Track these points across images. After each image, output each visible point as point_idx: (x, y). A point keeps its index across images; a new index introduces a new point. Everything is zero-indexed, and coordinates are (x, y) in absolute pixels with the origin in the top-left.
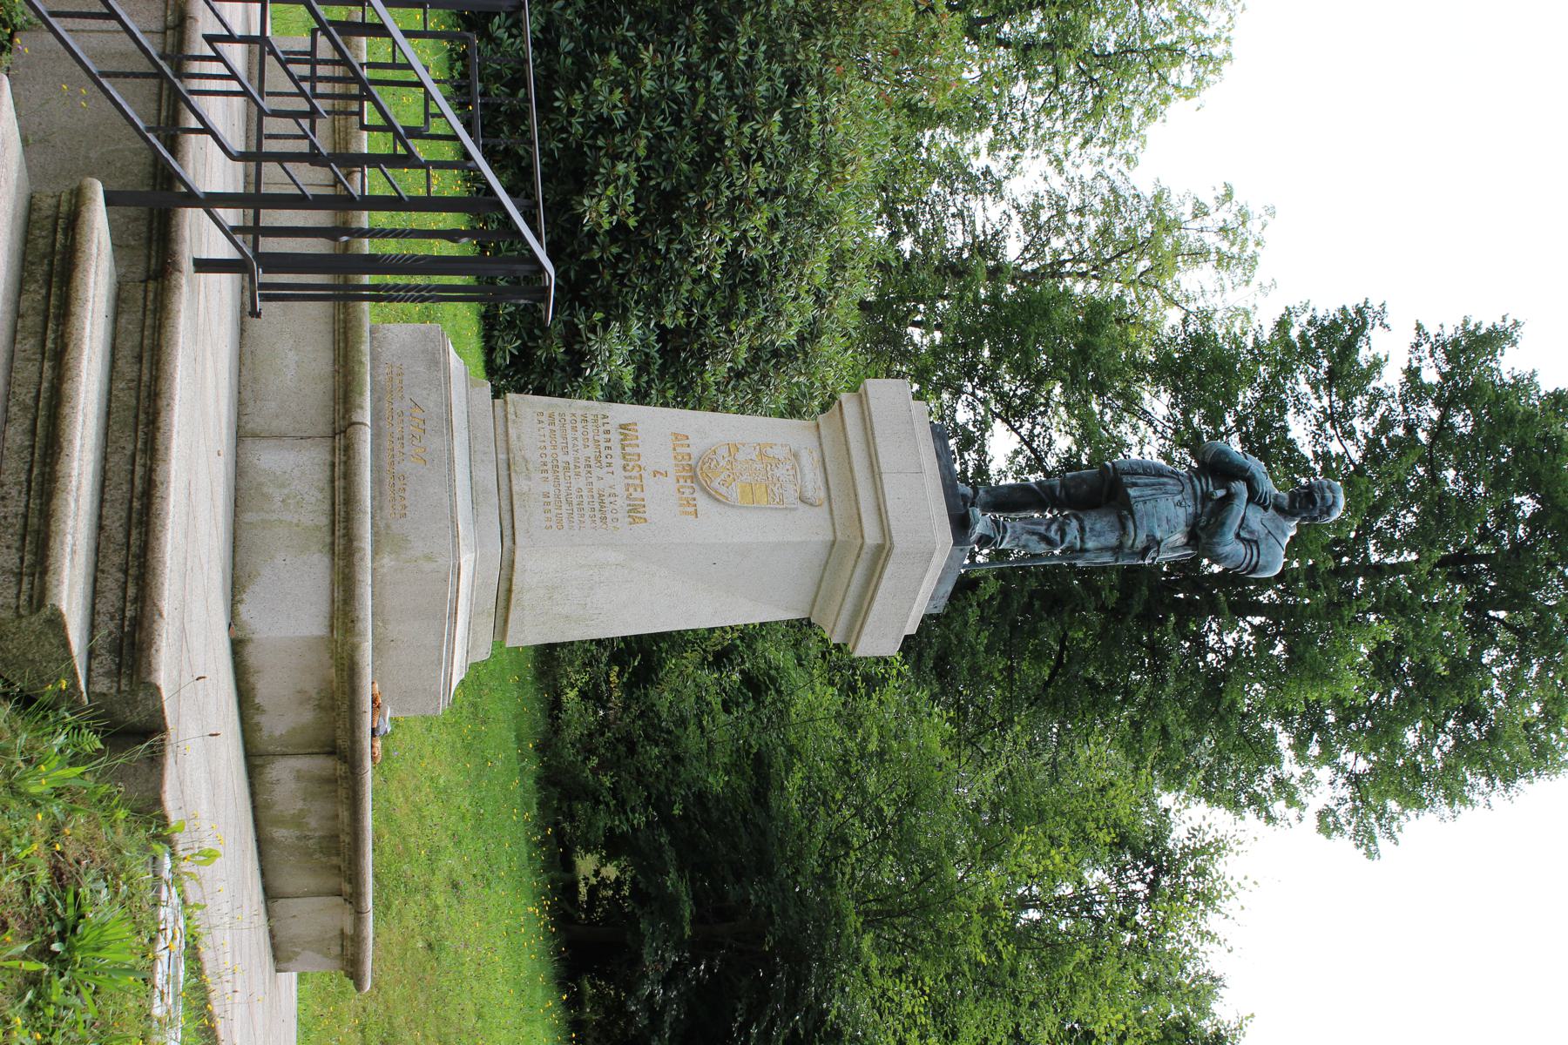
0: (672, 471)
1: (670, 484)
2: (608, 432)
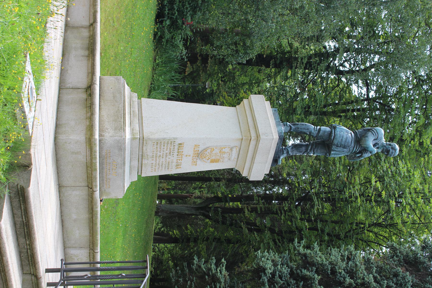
0: (192, 155)
1: (191, 158)
2: (174, 146)
